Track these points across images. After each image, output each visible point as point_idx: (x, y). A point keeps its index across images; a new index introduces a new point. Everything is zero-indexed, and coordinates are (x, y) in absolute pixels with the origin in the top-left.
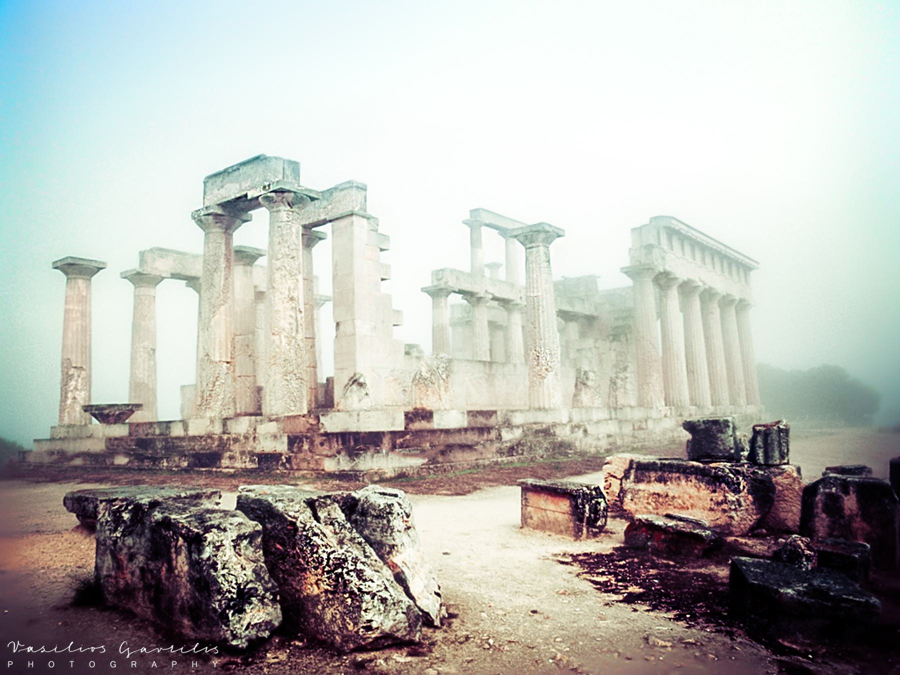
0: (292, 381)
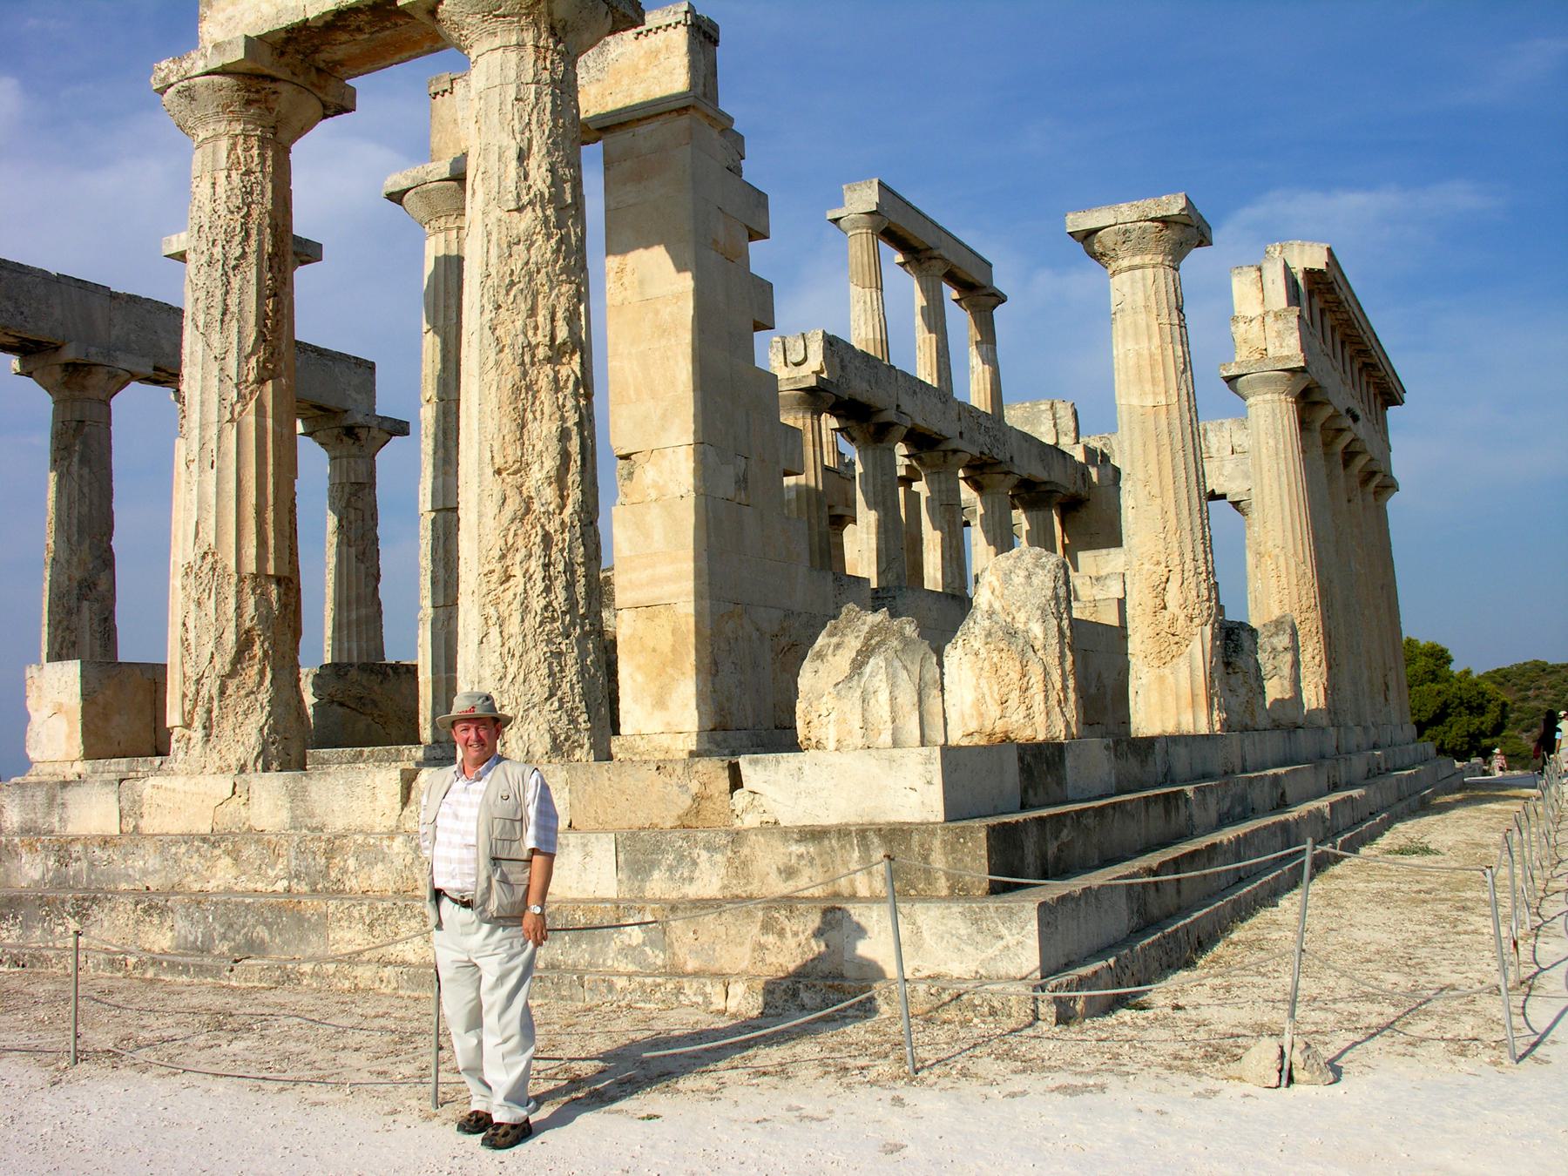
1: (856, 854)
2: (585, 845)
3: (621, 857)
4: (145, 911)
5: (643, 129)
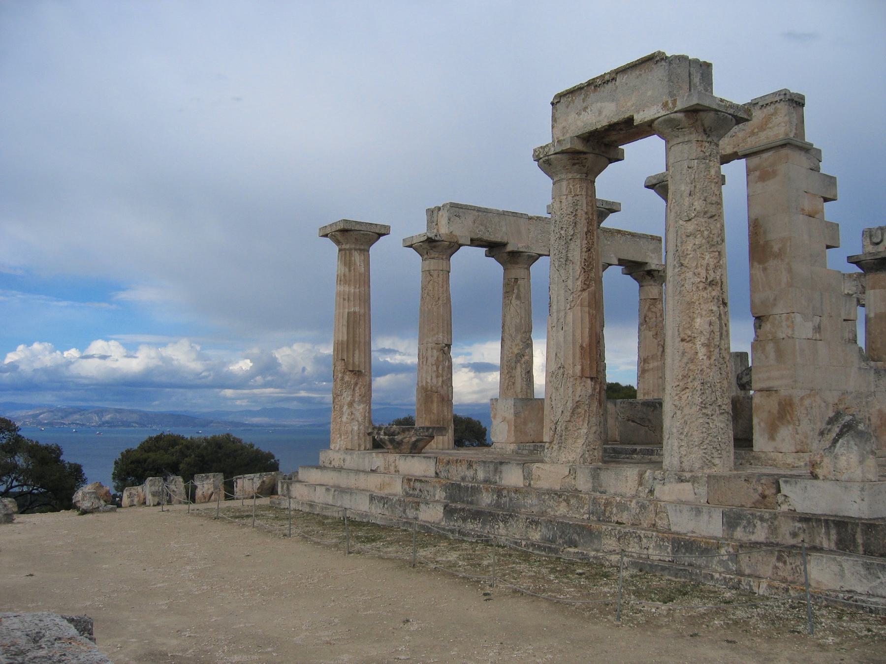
0: (714, 417)
1: (823, 530)
2: (710, 513)
3: (724, 520)
4: (529, 522)
5: (765, 156)
